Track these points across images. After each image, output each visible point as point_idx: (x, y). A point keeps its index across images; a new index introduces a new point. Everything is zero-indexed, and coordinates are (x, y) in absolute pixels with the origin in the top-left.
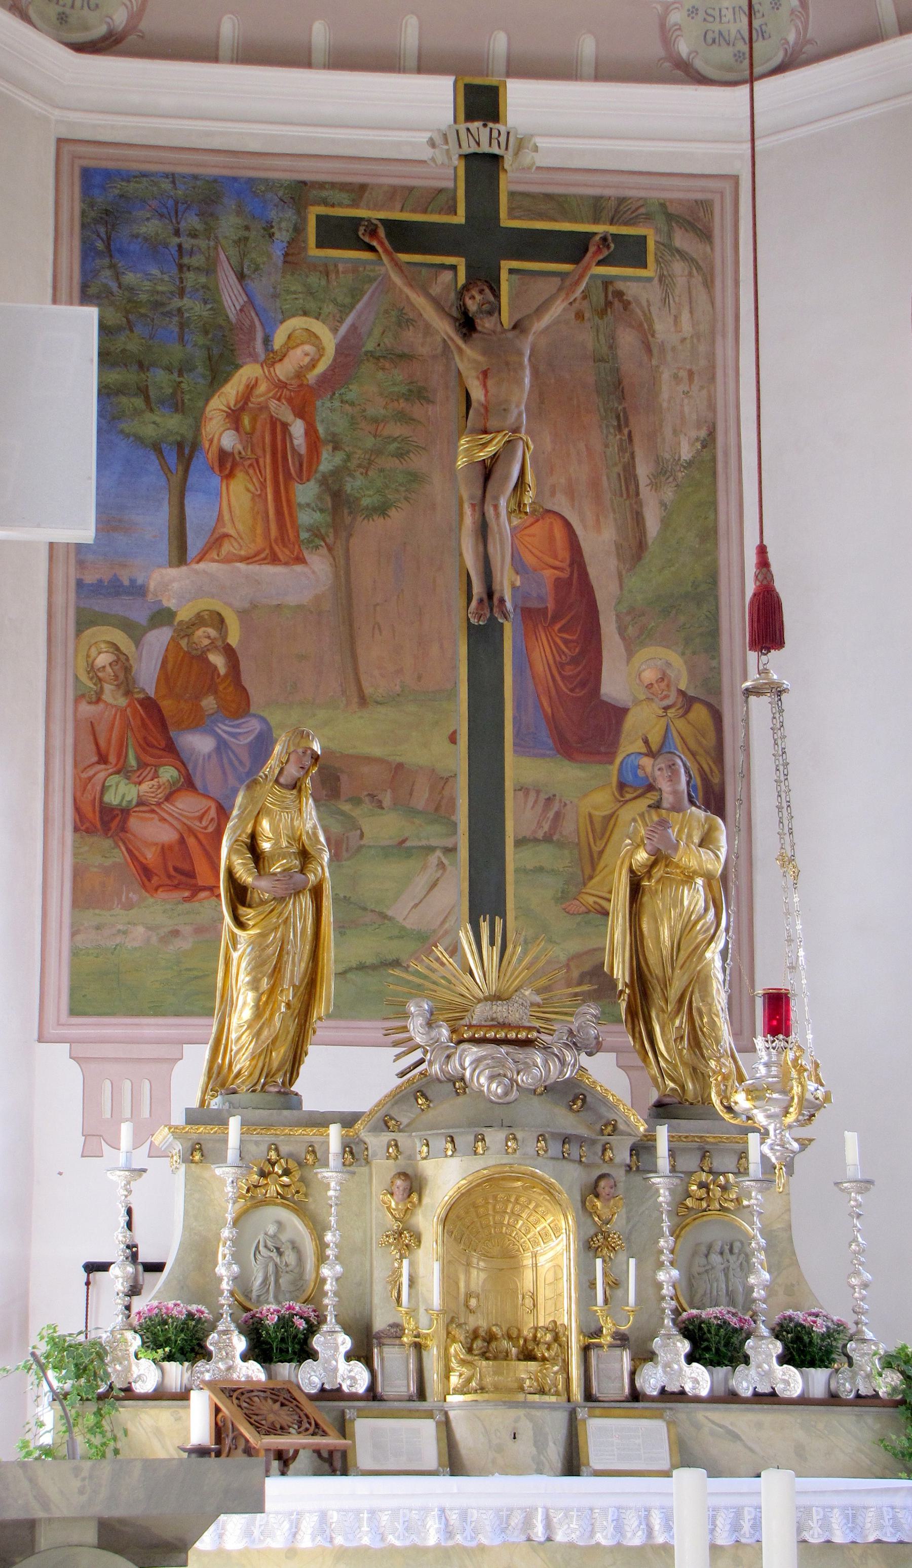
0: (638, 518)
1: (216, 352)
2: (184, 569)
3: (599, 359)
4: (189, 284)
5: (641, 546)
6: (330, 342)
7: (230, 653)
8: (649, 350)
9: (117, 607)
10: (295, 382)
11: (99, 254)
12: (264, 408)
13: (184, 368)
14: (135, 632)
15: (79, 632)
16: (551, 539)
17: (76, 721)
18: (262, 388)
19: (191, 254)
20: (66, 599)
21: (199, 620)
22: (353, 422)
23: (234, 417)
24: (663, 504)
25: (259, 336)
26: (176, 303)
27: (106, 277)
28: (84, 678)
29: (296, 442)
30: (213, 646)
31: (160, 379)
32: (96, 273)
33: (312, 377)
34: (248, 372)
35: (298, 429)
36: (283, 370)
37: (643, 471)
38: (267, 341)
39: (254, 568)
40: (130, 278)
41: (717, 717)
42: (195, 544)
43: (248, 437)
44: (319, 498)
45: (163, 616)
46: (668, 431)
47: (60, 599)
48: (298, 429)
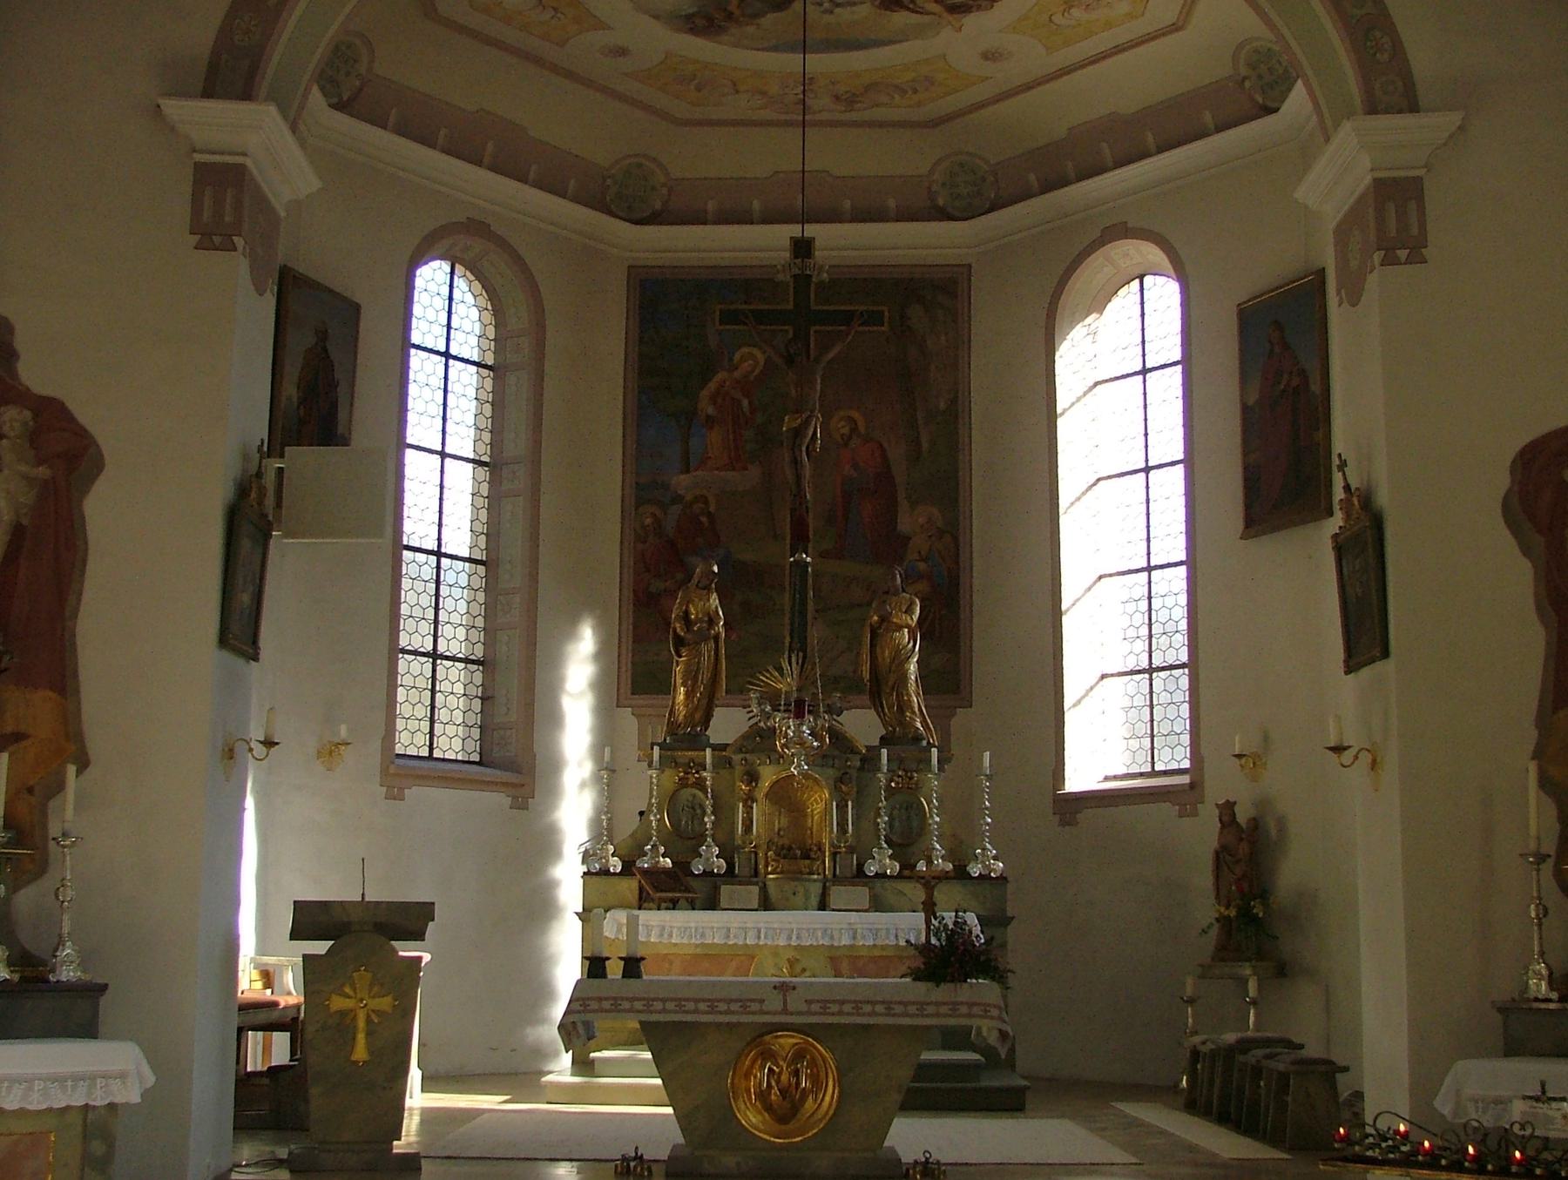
2: (688, 475)
6: (761, 357)
7: (710, 515)
23: (713, 399)
29: (744, 410)
34: (720, 376)
35: (745, 403)
36: (737, 374)
38: (731, 359)
45: (677, 499)
48: (745, 403)
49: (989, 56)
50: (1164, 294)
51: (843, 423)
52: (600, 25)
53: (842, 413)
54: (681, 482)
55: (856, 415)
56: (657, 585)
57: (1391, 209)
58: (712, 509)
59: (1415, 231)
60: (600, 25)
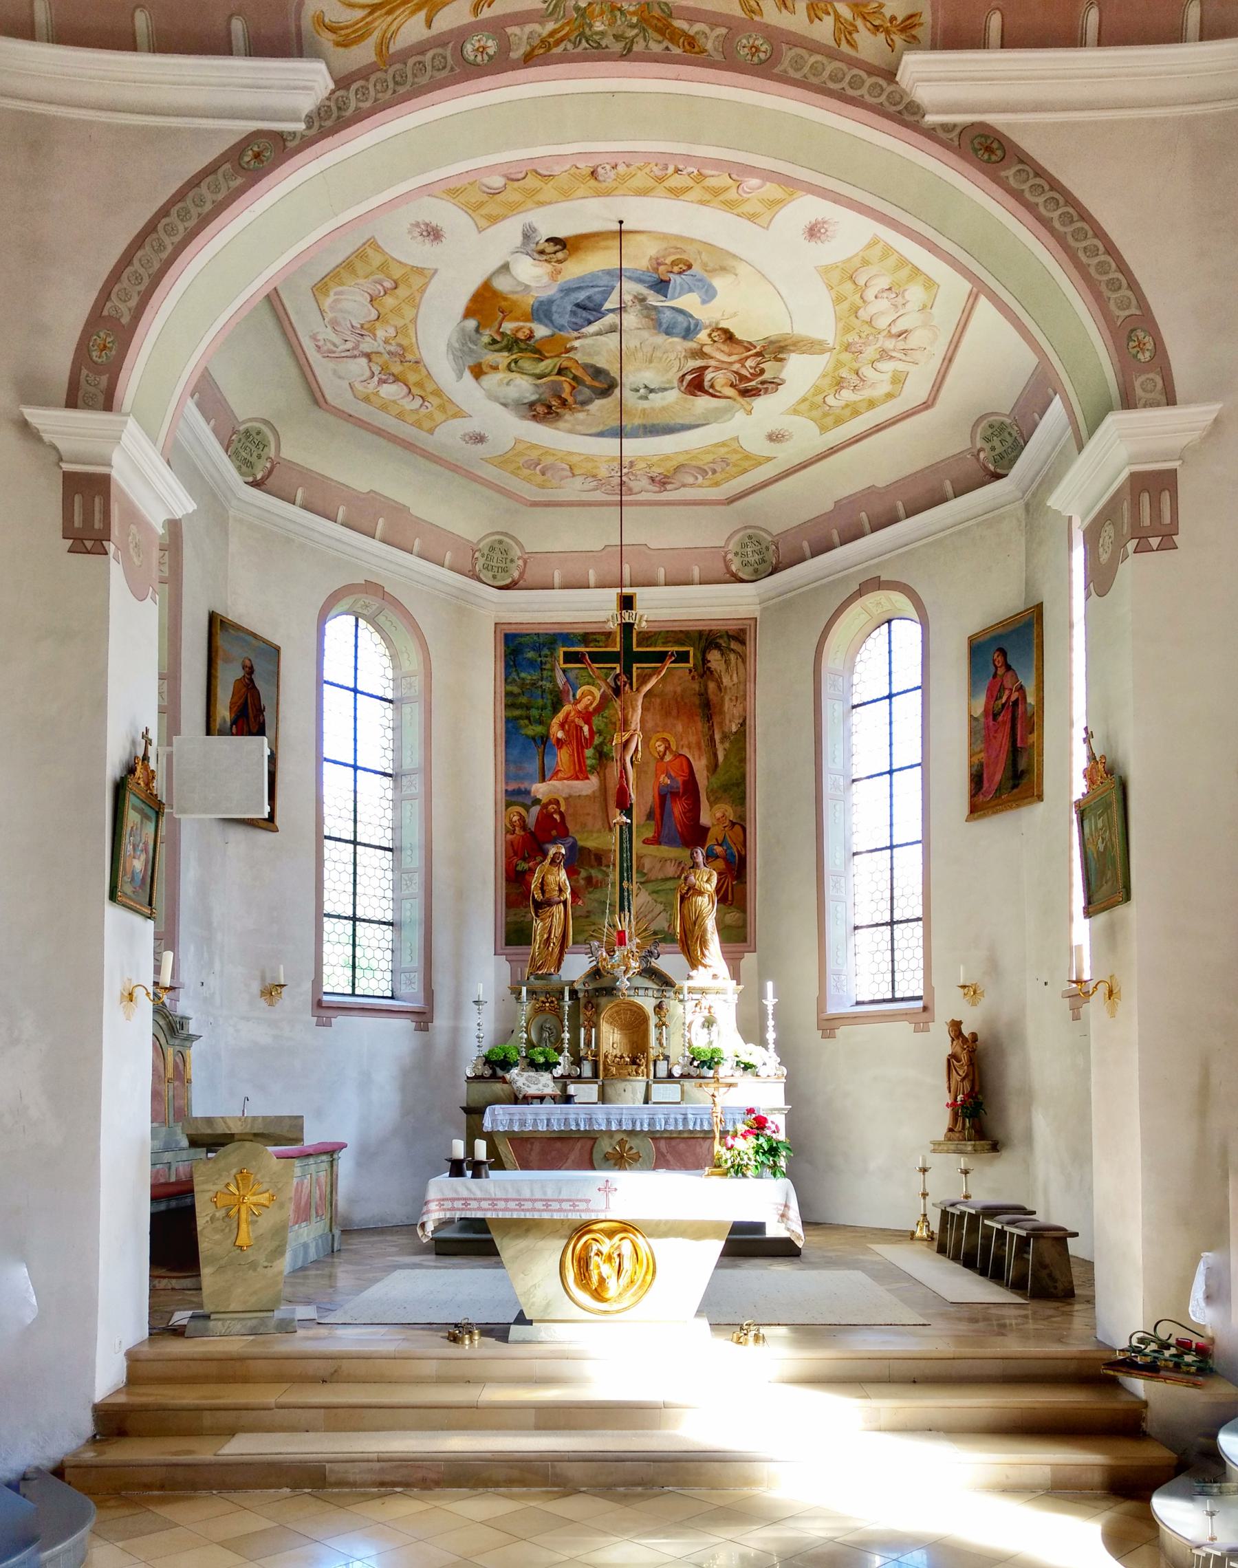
0: (715, 755)
1: (555, 700)
3: (700, 695)
4: (545, 675)
5: (716, 765)
6: (598, 694)
7: (561, 814)
8: (720, 690)
9: (520, 799)
10: (584, 711)
11: (511, 666)
12: (573, 721)
13: (543, 708)
14: (527, 809)
15: (506, 809)
16: (682, 765)
17: (506, 842)
18: (573, 714)
19: (545, 664)
20: (502, 797)
21: (550, 803)
22: (606, 725)
23: (562, 725)
24: (725, 749)
25: (571, 693)
26: (540, 683)
27: (514, 675)
28: (508, 825)
30: (555, 812)
31: (534, 713)
32: (510, 674)
33: (591, 709)
34: (567, 708)
35: (586, 728)
37: (717, 737)
38: (574, 695)
39: (570, 782)
40: (523, 675)
41: (744, 830)
42: (548, 775)
43: (567, 733)
44: (594, 754)
45: (537, 801)
46: (727, 722)
47: (499, 796)
48: (586, 728)
49: (774, 437)
50: (908, 633)
51: (658, 743)
52: (459, 414)
53: (660, 735)
54: (540, 790)
55: (666, 735)
56: (523, 866)
57: (1145, 498)
58: (562, 809)
59: (1167, 518)
60: (459, 414)
